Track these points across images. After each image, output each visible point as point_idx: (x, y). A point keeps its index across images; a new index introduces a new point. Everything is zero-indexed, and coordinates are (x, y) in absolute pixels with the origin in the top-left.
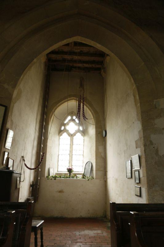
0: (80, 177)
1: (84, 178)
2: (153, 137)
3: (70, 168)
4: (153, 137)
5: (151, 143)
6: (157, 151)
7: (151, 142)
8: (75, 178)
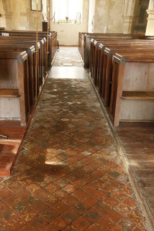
0: (73, 22)
1: (75, 23)
2: (98, 9)
3: (67, 16)
4: (98, 9)
6: (98, 15)
7: (97, 11)
8: (70, 23)
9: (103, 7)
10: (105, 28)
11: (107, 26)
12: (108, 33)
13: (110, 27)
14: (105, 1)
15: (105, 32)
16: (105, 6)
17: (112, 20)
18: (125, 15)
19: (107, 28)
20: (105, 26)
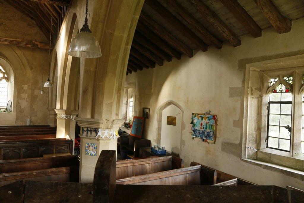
2: (20, 101)
4: (20, 101)
5: (19, 103)
7: (19, 102)
9: (25, 99)
10: (28, 120)
11: (30, 118)
12: (32, 125)
13: (33, 118)
14: (27, 95)
15: (28, 125)
16: (28, 99)
17: (37, 112)
18: (50, 107)
19: (31, 120)
20: (28, 118)
